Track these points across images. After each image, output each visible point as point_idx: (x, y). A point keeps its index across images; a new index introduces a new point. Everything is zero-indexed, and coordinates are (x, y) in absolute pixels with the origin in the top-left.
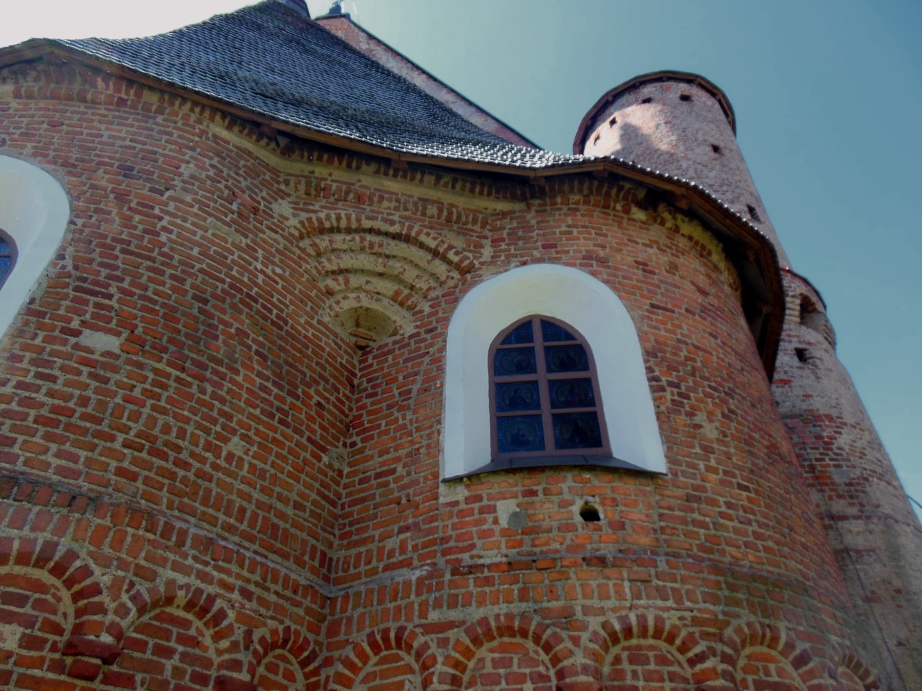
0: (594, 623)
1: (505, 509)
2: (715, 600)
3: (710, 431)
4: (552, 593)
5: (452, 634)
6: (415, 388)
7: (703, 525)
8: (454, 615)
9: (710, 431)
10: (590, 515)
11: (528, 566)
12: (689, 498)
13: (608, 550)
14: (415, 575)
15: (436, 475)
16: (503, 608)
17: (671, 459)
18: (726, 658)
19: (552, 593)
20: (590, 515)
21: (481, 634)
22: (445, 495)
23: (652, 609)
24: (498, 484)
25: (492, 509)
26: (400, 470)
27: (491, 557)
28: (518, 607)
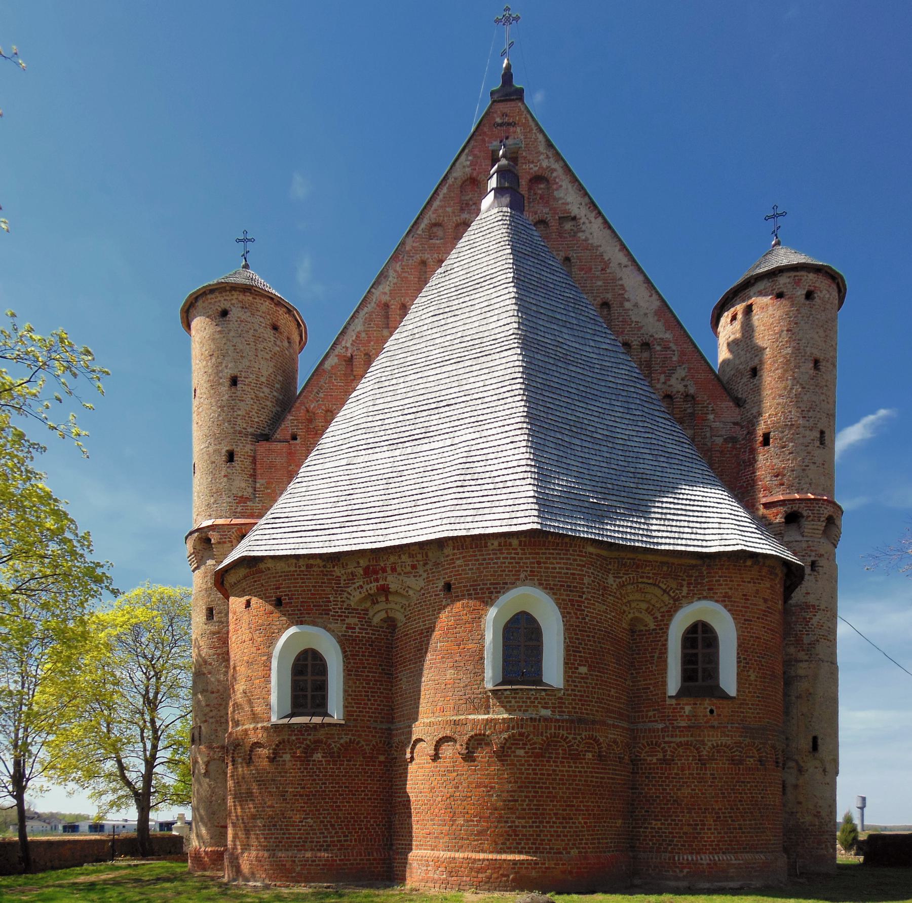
0: (710, 744)
1: (688, 709)
2: (741, 736)
3: (753, 678)
4: (700, 736)
5: (672, 745)
6: (656, 655)
7: (743, 712)
8: (674, 739)
9: (753, 678)
10: (712, 711)
11: (693, 727)
12: (741, 704)
13: (716, 724)
14: (660, 726)
15: (665, 693)
16: (686, 739)
17: (738, 691)
18: (741, 752)
19: (700, 736)
20: (712, 711)
21: (680, 745)
22: (668, 702)
23: (724, 740)
24: (684, 700)
25: (683, 708)
26: (652, 689)
27: (683, 724)
28: (690, 739)
